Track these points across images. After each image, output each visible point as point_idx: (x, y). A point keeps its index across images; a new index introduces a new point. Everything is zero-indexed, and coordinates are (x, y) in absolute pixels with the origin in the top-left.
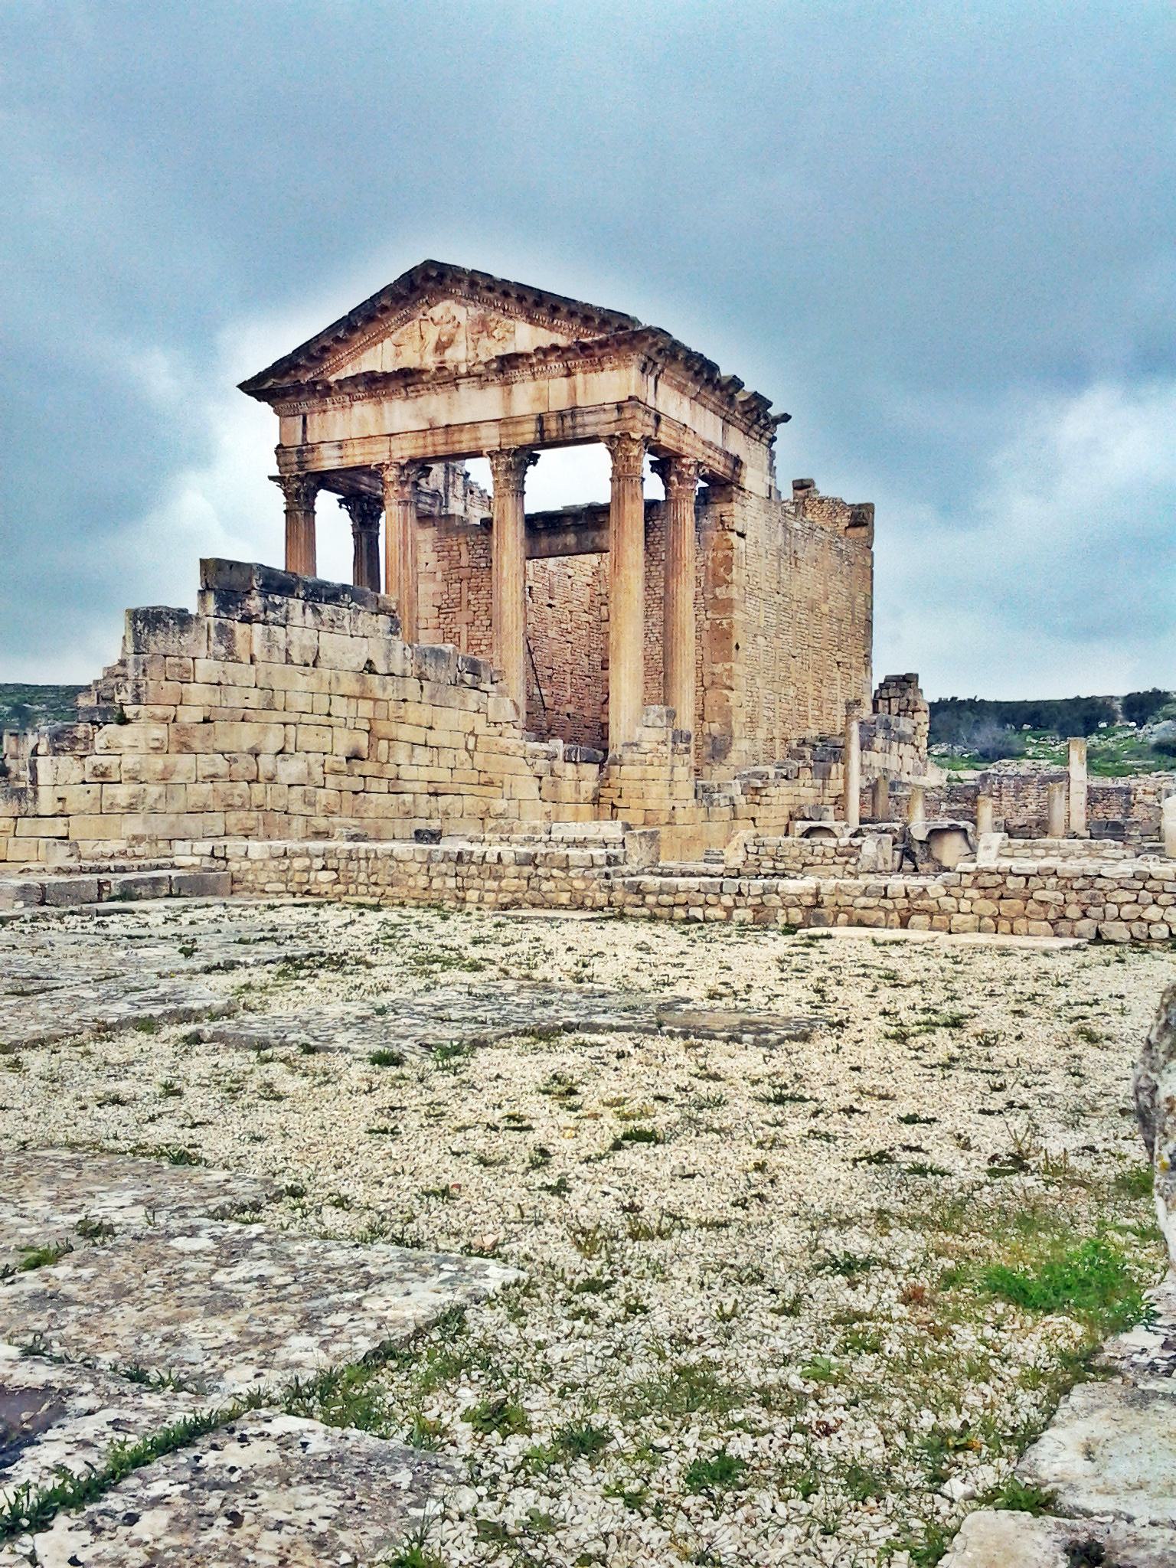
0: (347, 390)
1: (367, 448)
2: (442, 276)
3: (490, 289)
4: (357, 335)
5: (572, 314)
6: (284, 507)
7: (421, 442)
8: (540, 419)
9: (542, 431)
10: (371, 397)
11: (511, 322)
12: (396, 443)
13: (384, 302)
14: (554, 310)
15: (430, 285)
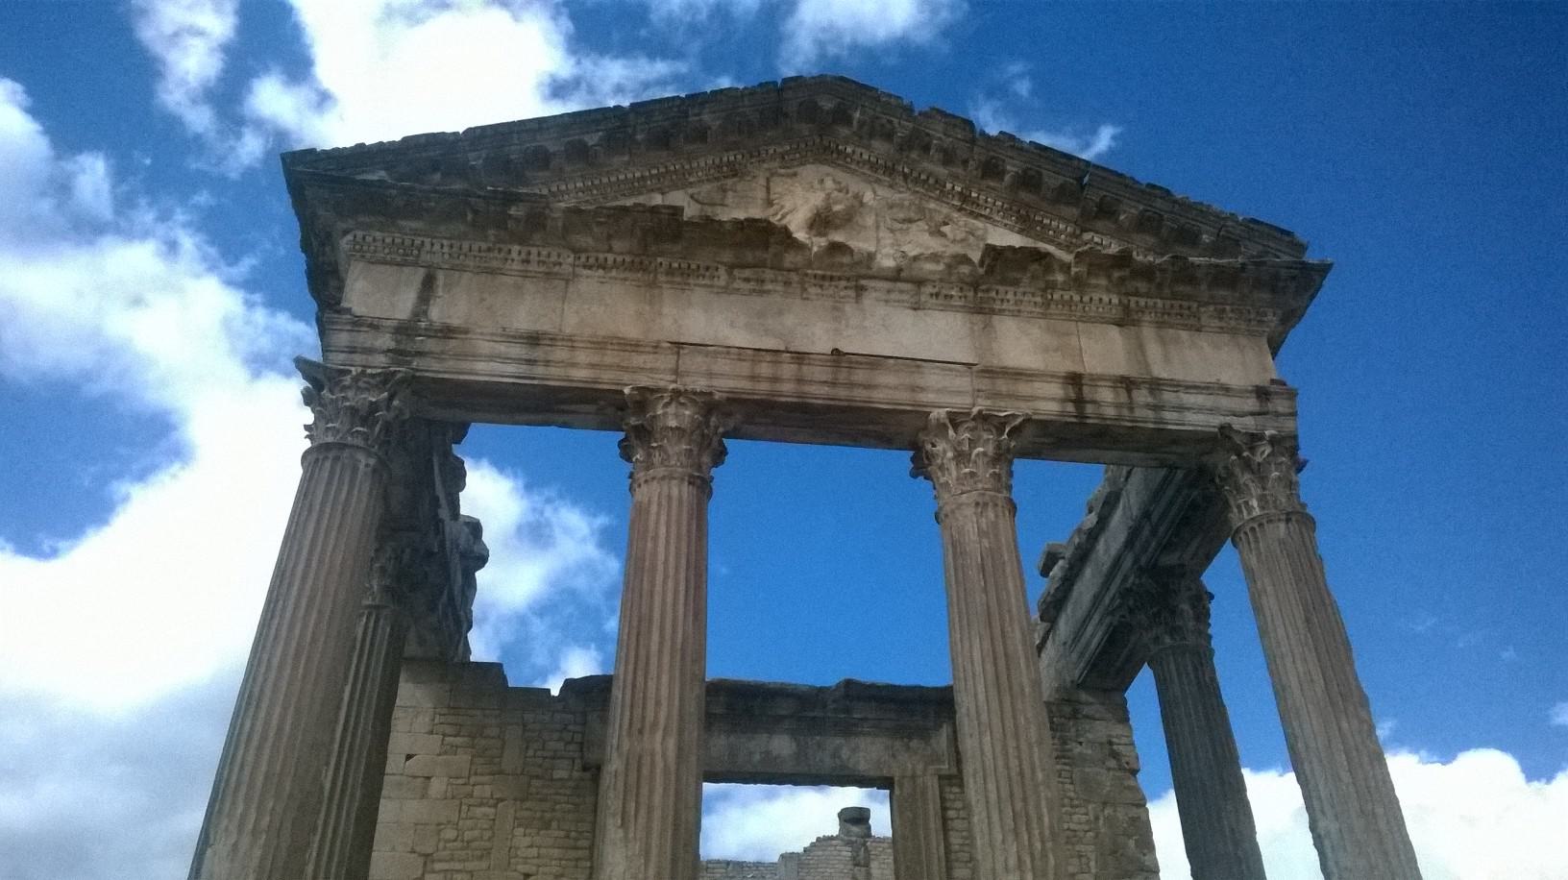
0: (584, 240)
1: (610, 357)
2: (842, 116)
3: (948, 158)
4: (618, 160)
5: (1146, 223)
6: (307, 444)
7: (765, 369)
8: (1075, 380)
9: (1079, 401)
10: (631, 267)
11: (979, 224)
12: (692, 362)
13: (706, 117)
14: (1106, 211)
15: (805, 128)
